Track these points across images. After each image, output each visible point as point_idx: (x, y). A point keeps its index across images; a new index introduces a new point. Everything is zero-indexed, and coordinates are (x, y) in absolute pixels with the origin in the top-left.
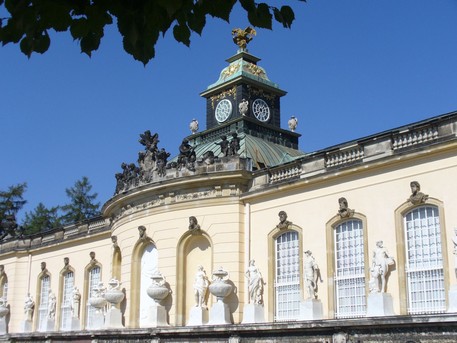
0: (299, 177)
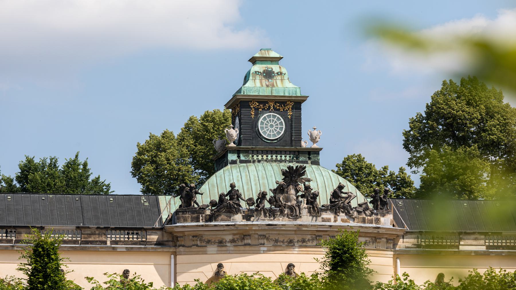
0: (458, 247)
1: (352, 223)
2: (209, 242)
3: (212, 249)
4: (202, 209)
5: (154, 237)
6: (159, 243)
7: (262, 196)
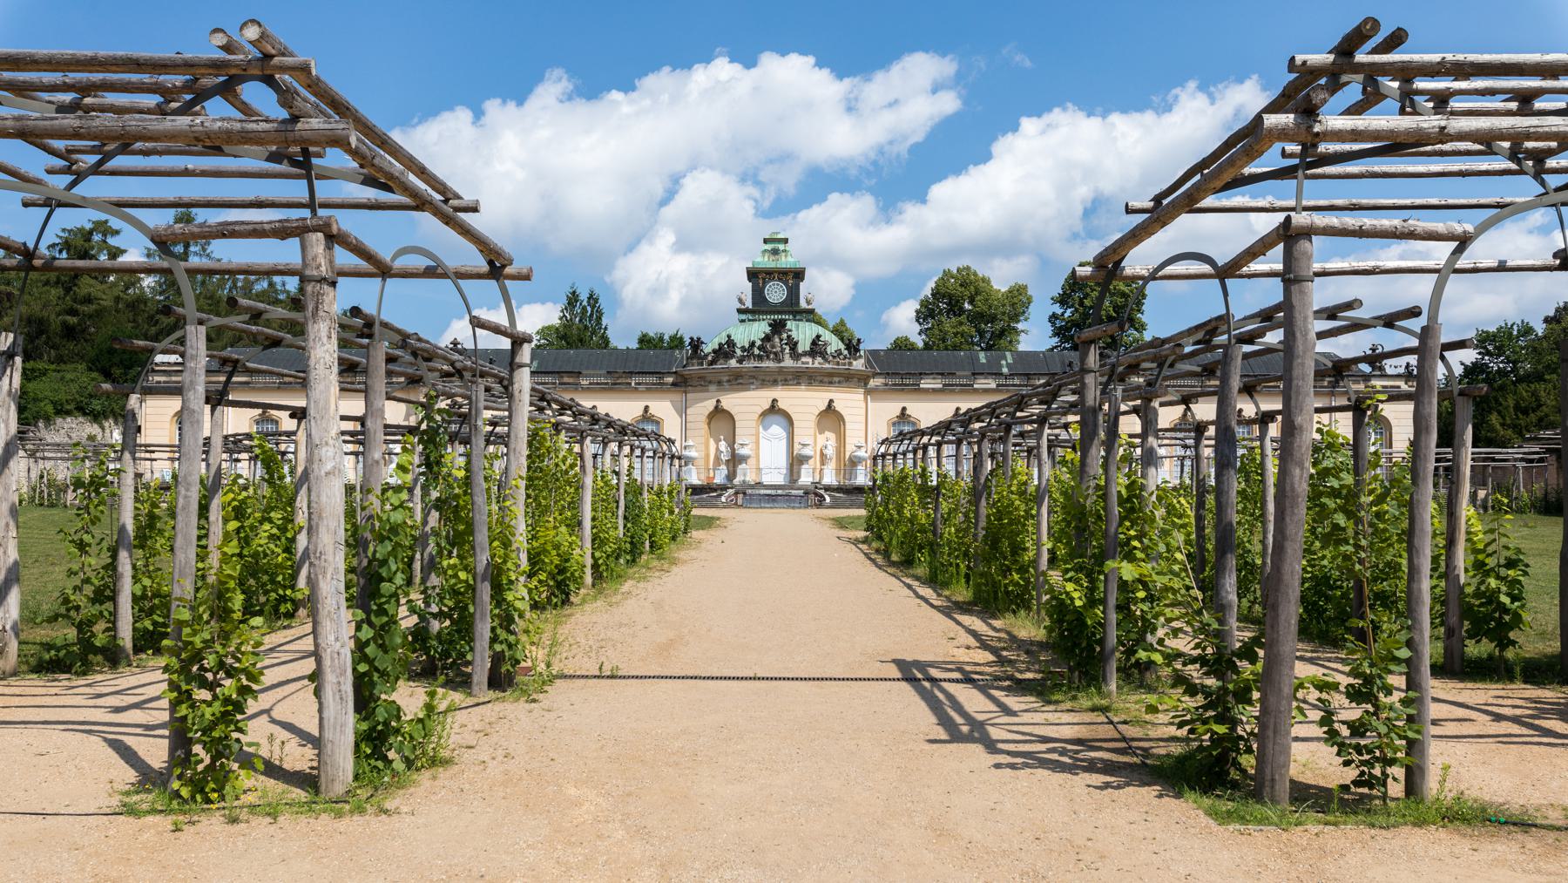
1: (827, 366)
2: (710, 382)
3: (713, 387)
4: (707, 355)
5: (670, 380)
6: (674, 384)
7: (752, 344)
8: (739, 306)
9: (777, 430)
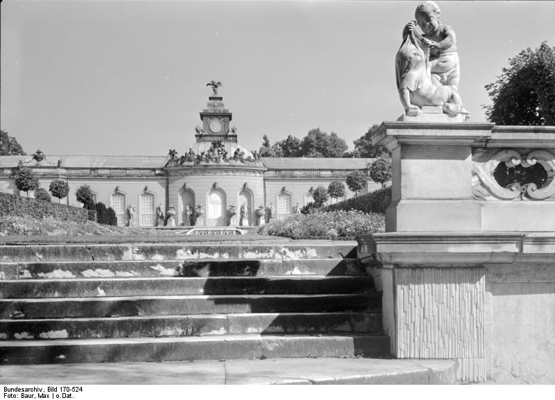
7: (203, 154)
8: (196, 133)
9: (216, 197)
